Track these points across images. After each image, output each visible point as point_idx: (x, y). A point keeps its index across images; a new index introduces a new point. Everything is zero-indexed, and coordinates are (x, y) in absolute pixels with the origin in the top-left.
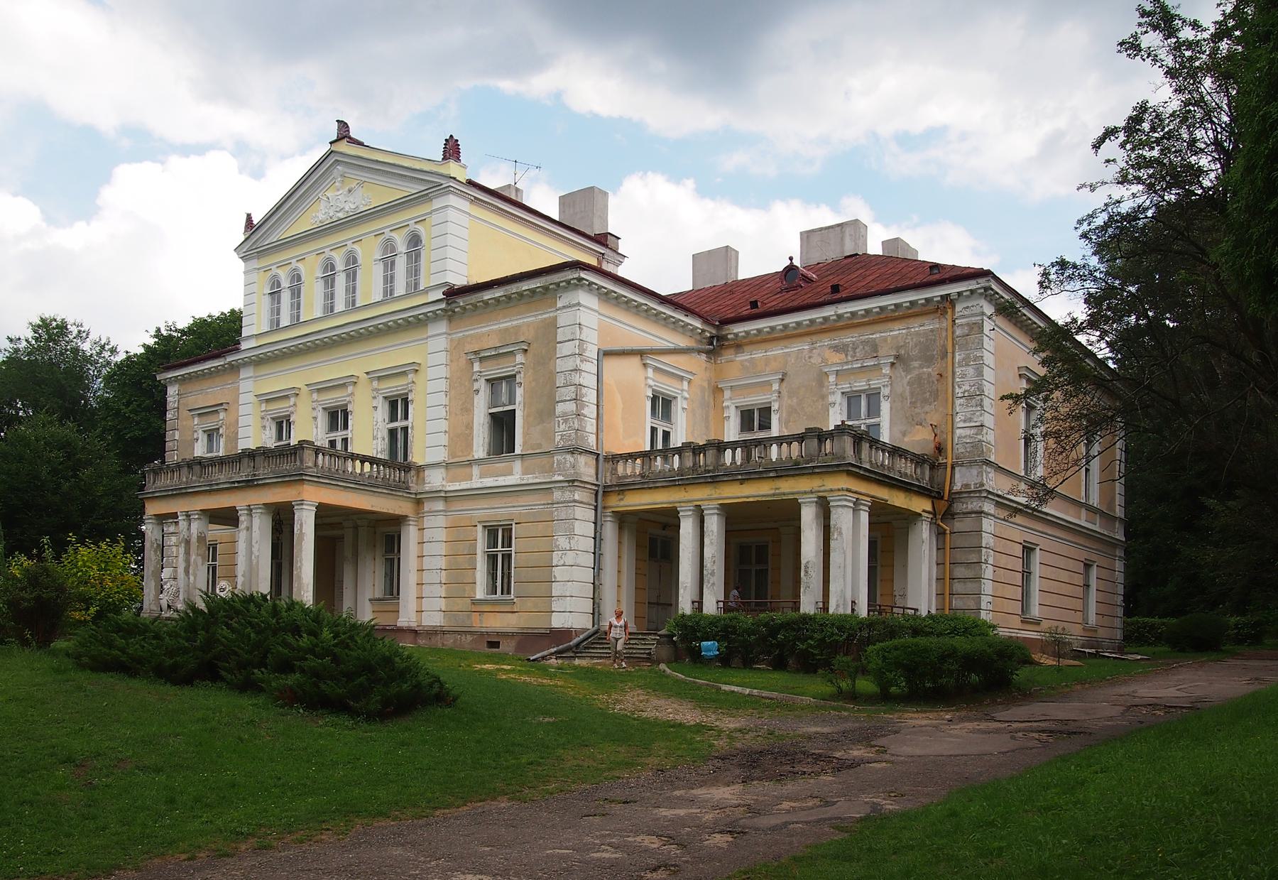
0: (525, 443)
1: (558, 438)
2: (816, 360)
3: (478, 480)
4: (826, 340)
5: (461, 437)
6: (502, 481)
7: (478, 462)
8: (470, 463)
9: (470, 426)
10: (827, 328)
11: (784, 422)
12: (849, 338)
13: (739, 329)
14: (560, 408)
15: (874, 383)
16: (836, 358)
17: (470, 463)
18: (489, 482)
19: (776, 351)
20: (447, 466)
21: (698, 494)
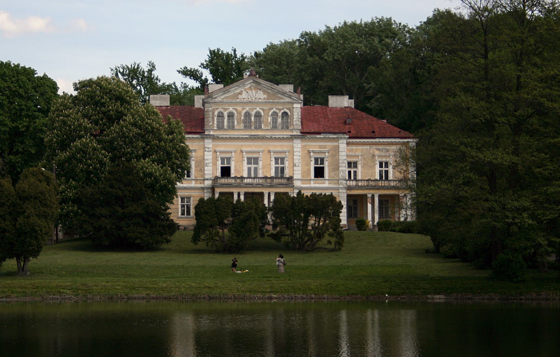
0: (329, 177)
1: (340, 176)
2: (371, 152)
3: (313, 185)
4: (374, 147)
5: (305, 173)
6: (322, 185)
7: (313, 180)
8: (310, 180)
9: (309, 170)
10: (376, 144)
11: (363, 167)
12: (380, 147)
13: (351, 140)
14: (340, 169)
15: (388, 160)
16: (377, 153)
17: (310, 180)
18: (317, 185)
19: (360, 147)
20: (301, 180)
21: (372, 192)
